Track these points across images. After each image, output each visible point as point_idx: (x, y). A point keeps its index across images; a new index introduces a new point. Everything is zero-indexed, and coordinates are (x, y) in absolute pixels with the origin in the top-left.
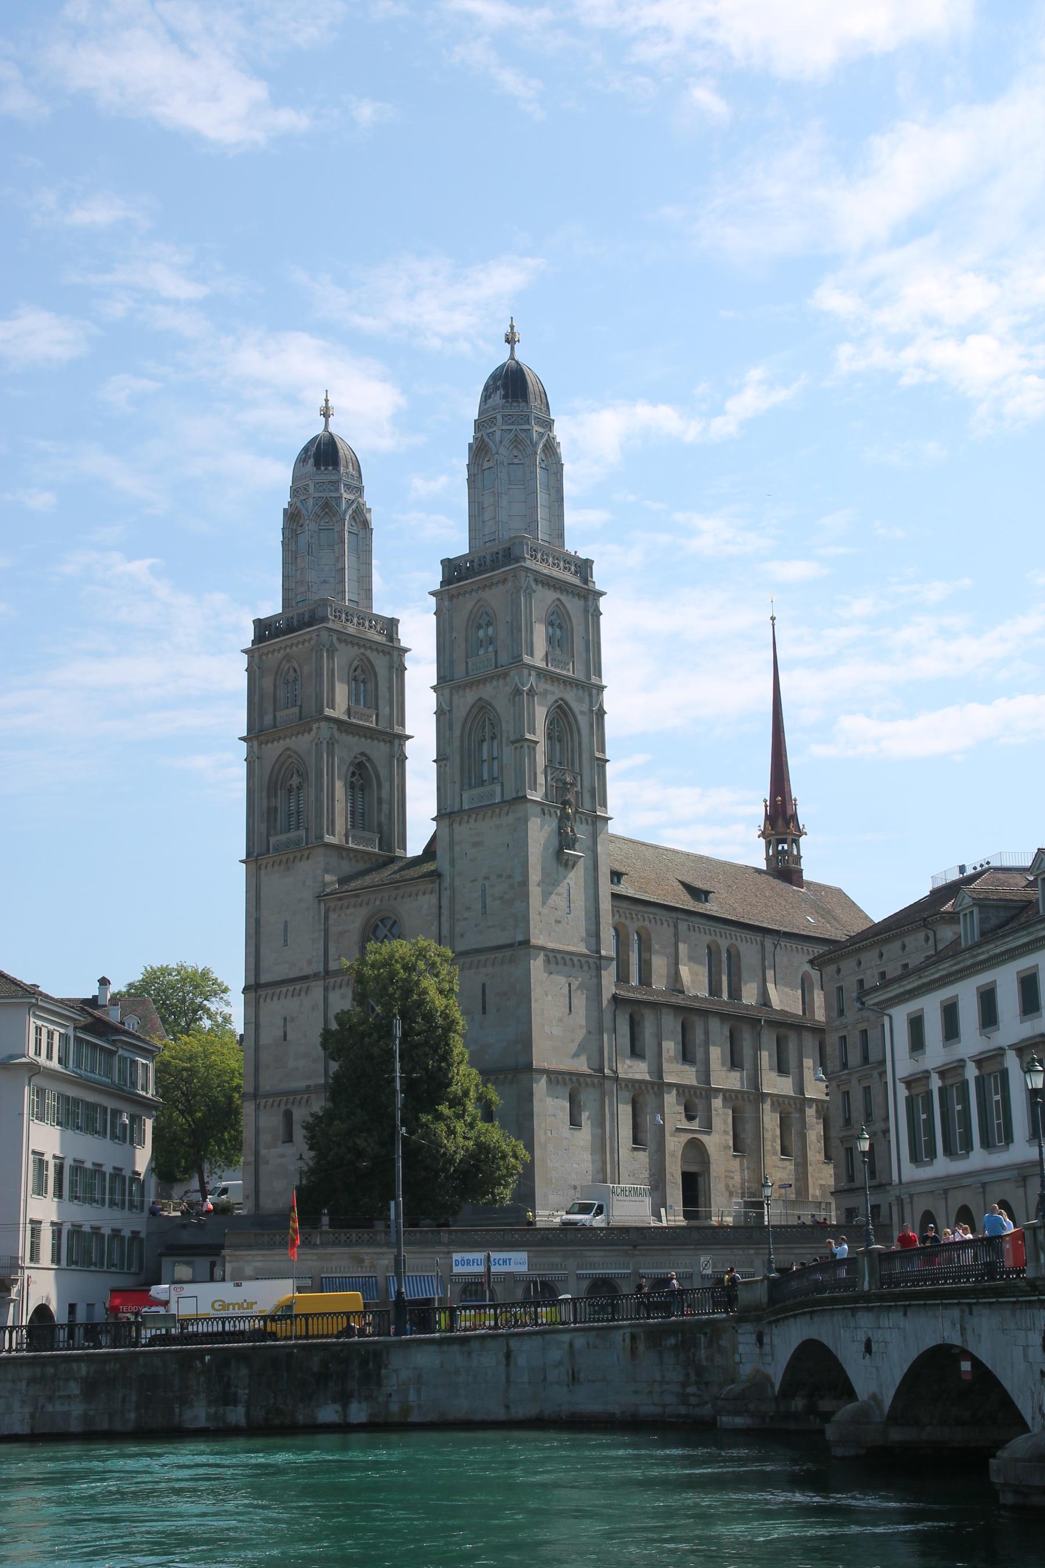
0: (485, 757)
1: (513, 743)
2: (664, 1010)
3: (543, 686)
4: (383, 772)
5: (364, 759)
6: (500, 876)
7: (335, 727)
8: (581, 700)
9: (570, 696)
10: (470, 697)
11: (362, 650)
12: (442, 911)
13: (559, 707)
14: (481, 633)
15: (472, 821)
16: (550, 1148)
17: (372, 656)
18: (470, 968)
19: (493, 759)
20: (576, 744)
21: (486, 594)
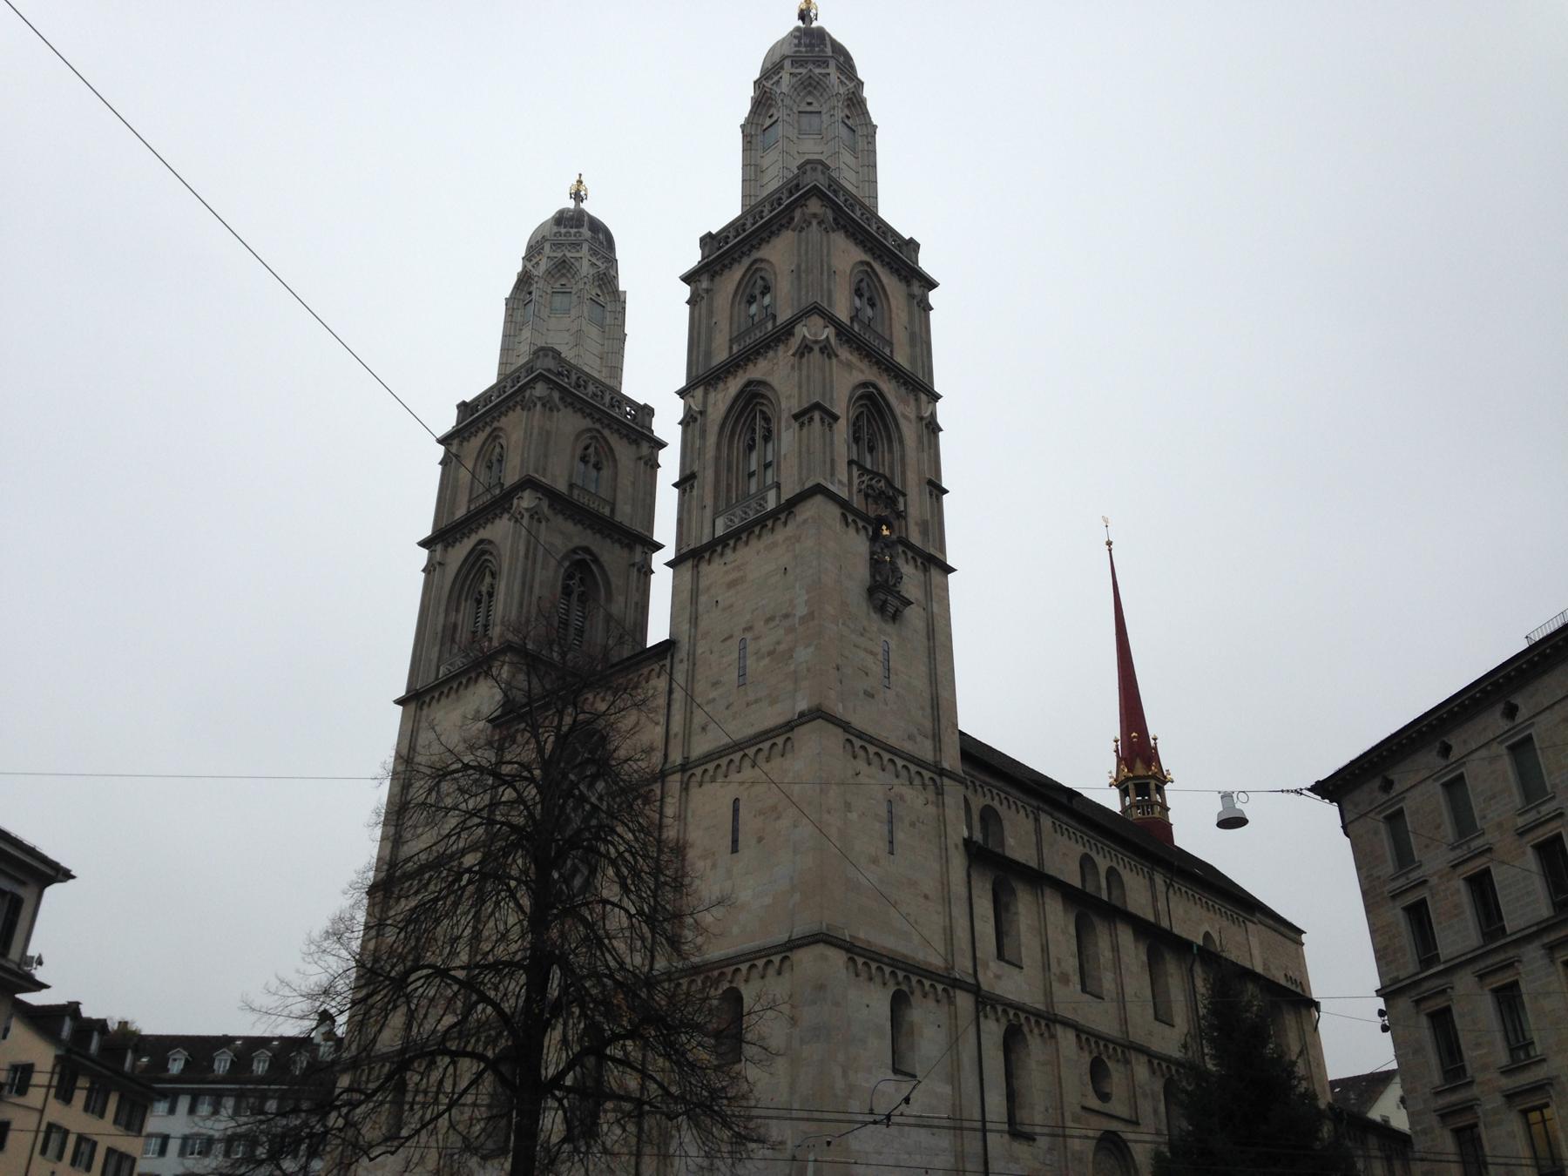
0: (754, 467)
1: (796, 417)
2: (1048, 891)
3: (844, 353)
4: (616, 581)
5: (588, 557)
6: (770, 619)
8: (906, 403)
9: (888, 387)
10: (734, 386)
11: (598, 426)
13: (870, 397)
14: (754, 309)
15: (728, 551)
17: (614, 440)
18: (713, 780)
19: (767, 466)
20: (897, 455)
21: (765, 252)
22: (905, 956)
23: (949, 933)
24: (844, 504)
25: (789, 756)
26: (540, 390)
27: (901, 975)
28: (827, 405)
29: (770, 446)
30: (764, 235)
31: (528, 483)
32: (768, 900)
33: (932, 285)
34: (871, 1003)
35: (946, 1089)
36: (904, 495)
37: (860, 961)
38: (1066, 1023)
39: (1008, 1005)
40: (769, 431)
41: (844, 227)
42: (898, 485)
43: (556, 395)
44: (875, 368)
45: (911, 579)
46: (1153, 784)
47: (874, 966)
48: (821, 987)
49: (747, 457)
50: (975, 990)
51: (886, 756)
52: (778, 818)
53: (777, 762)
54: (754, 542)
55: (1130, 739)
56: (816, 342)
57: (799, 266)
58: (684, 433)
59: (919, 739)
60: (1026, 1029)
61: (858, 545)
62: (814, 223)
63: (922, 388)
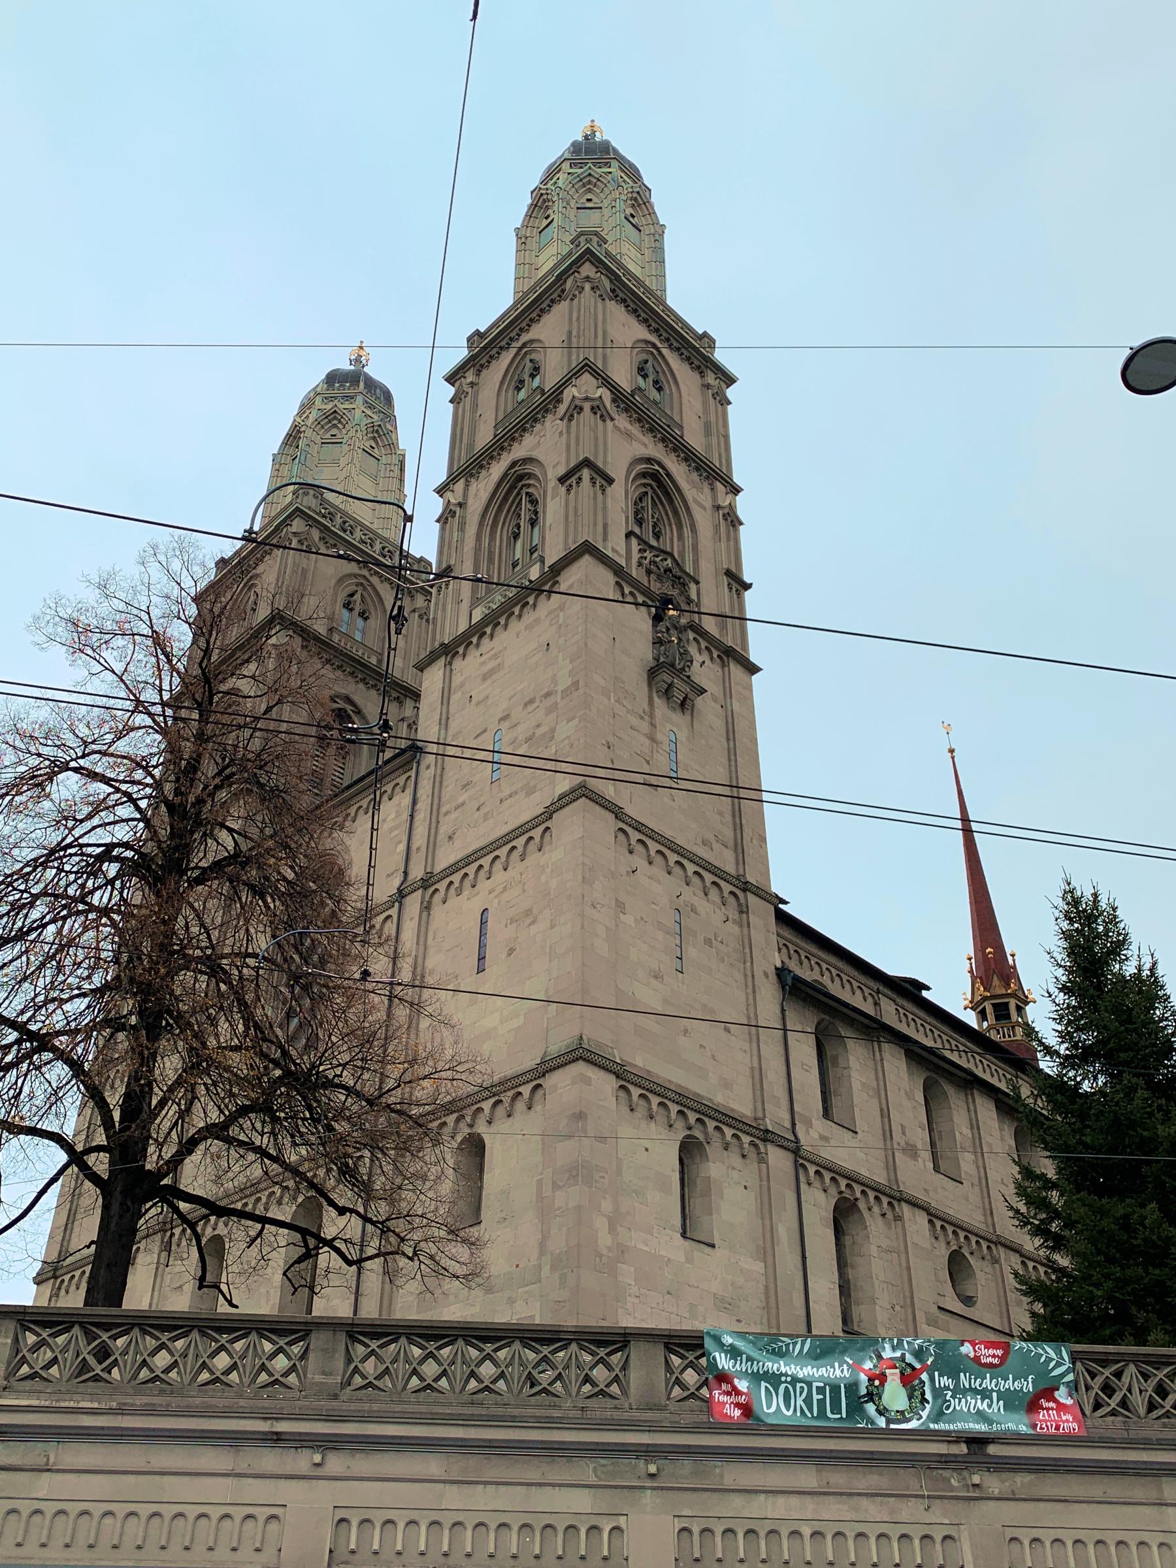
0: (518, 555)
1: (562, 480)
3: (622, 421)
5: (349, 708)
6: (531, 701)
7: (298, 641)
9: (678, 469)
10: (497, 470)
11: (365, 572)
12: (418, 807)
13: (655, 476)
14: (522, 395)
15: (485, 641)
16: (627, 1273)
20: (688, 541)
21: (535, 332)
22: (695, 1094)
23: (758, 1076)
24: (618, 571)
25: (546, 848)
26: (298, 525)
27: (692, 1117)
28: (600, 465)
29: (536, 530)
30: (534, 315)
31: (276, 618)
32: (515, 1023)
33: (730, 380)
34: (654, 1148)
35: (759, 1267)
36: (697, 583)
37: (636, 1092)
38: (914, 1204)
39: (837, 1173)
40: (536, 513)
41: (624, 301)
42: (689, 568)
43: (316, 534)
44: (661, 445)
45: (704, 670)
46: (1013, 1003)
47: (655, 1100)
48: (580, 1116)
49: (511, 547)
50: (795, 1150)
51: (673, 858)
52: (533, 922)
53: (533, 857)
54: (514, 624)
55: (985, 955)
56: (587, 399)
57: (570, 332)
58: (443, 529)
59: (715, 846)
60: (862, 1205)
61: (640, 621)
62: (587, 286)
63: (717, 476)
